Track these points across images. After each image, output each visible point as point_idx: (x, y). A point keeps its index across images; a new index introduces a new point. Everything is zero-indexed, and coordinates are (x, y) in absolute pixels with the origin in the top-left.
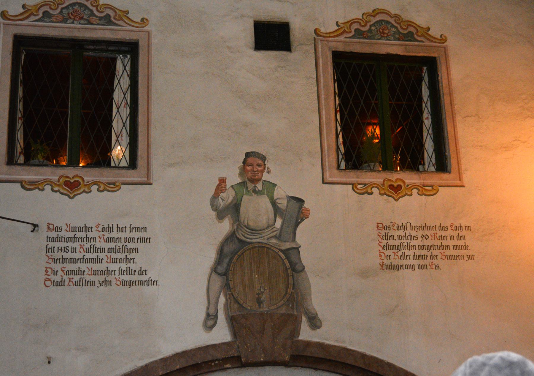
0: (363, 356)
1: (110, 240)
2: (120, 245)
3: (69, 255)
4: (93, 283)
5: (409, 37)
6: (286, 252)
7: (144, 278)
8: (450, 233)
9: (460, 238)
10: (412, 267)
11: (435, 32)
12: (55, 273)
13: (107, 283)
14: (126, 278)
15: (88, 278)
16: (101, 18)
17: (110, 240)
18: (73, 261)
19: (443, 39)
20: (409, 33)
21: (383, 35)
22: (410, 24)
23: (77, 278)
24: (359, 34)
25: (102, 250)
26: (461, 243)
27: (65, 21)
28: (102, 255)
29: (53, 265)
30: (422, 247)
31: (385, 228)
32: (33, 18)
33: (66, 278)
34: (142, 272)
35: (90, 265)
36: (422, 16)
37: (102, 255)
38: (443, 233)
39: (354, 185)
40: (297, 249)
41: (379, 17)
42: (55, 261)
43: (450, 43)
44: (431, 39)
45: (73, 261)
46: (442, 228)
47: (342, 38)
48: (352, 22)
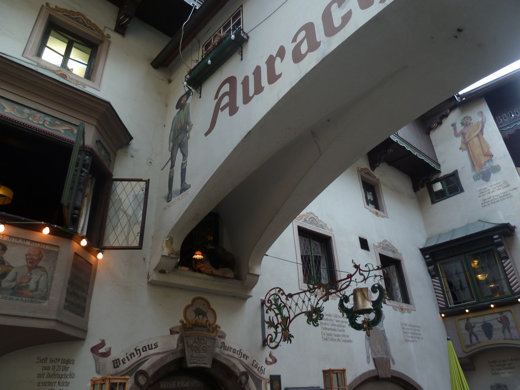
0: (407, 376)
1: (337, 321)
2: (340, 323)
3: (327, 327)
4: (335, 340)
5: (394, 252)
6: (382, 331)
7: (348, 339)
8: (416, 328)
9: (419, 331)
10: (411, 341)
11: (399, 251)
12: (324, 334)
13: (339, 340)
14: (344, 338)
15: (334, 338)
16: (320, 225)
17: (337, 321)
18: (329, 329)
19: (401, 255)
20: (394, 251)
21: (389, 250)
22: (394, 247)
23: (330, 337)
24: (383, 248)
25: (335, 325)
26: (419, 332)
27: (310, 224)
28: (336, 328)
29: (323, 331)
30: (412, 333)
31: (403, 325)
32: (302, 220)
33: (328, 337)
34: (348, 336)
35: (334, 332)
36: (396, 245)
37: (336, 328)
38: (415, 328)
39: (393, 306)
40: (384, 330)
41: (387, 243)
42: (324, 329)
43: (403, 256)
44: (398, 253)
45: (329, 329)
46: (415, 327)
47: (379, 249)
48: (381, 243)
